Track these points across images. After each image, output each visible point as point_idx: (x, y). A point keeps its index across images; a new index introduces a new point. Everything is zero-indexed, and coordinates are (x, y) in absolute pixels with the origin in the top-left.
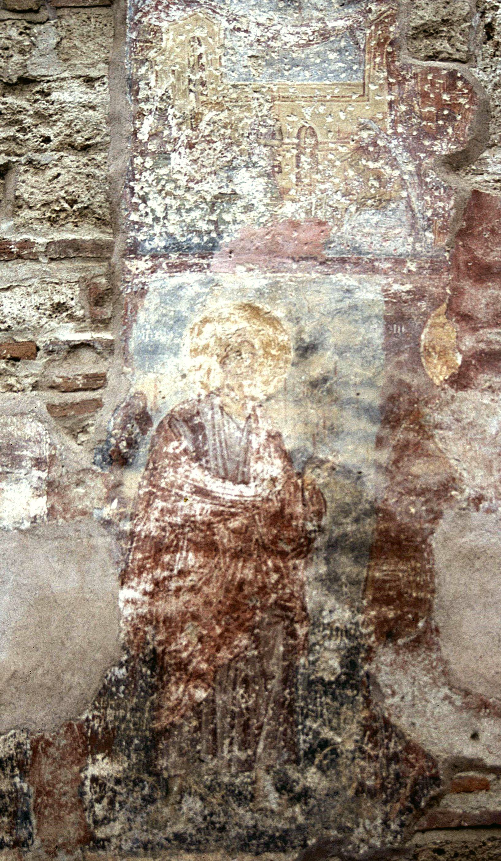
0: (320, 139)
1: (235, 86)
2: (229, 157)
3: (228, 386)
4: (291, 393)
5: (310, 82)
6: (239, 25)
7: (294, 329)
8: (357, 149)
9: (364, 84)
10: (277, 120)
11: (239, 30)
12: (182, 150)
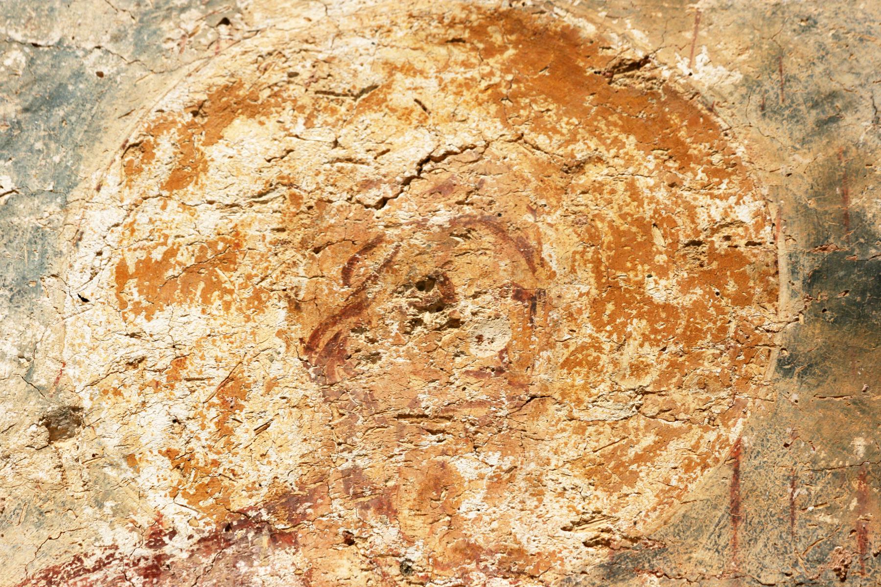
3: (352, 477)
4: (773, 533)
7: (802, 160)
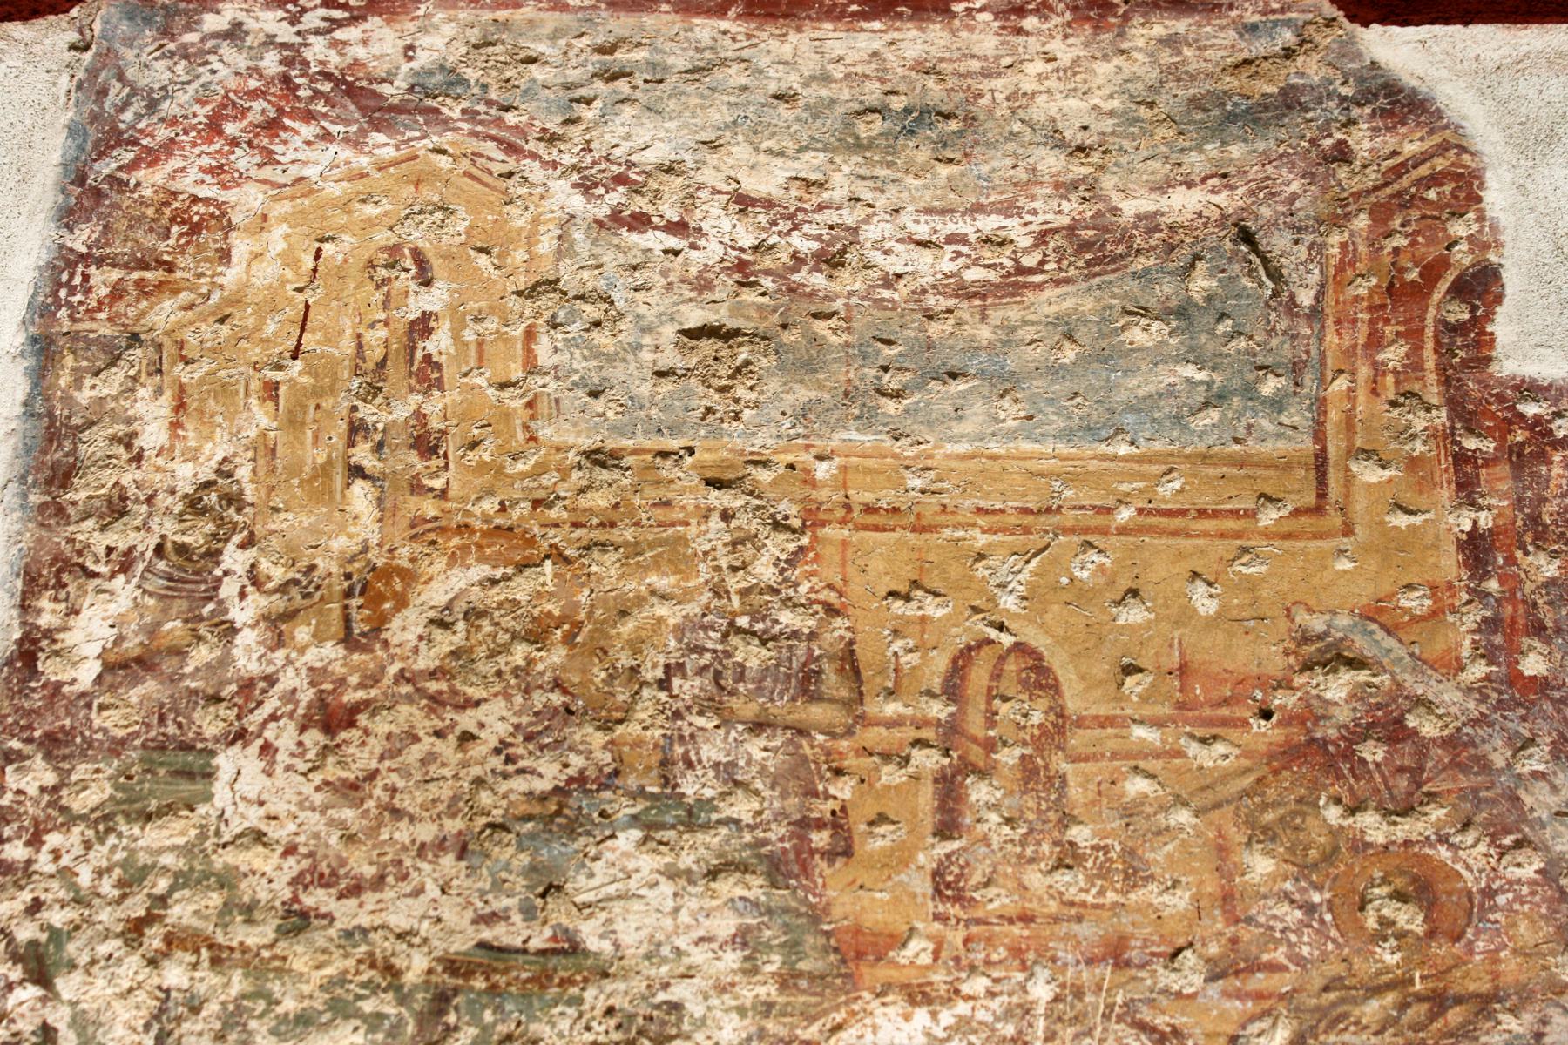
0: (1073, 704)
1: (598, 458)
2: (549, 773)
5: (1027, 446)
6: (641, 204)
8: (1289, 755)
9: (1320, 462)
10: (831, 611)
11: (640, 222)
12: (285, 737)
